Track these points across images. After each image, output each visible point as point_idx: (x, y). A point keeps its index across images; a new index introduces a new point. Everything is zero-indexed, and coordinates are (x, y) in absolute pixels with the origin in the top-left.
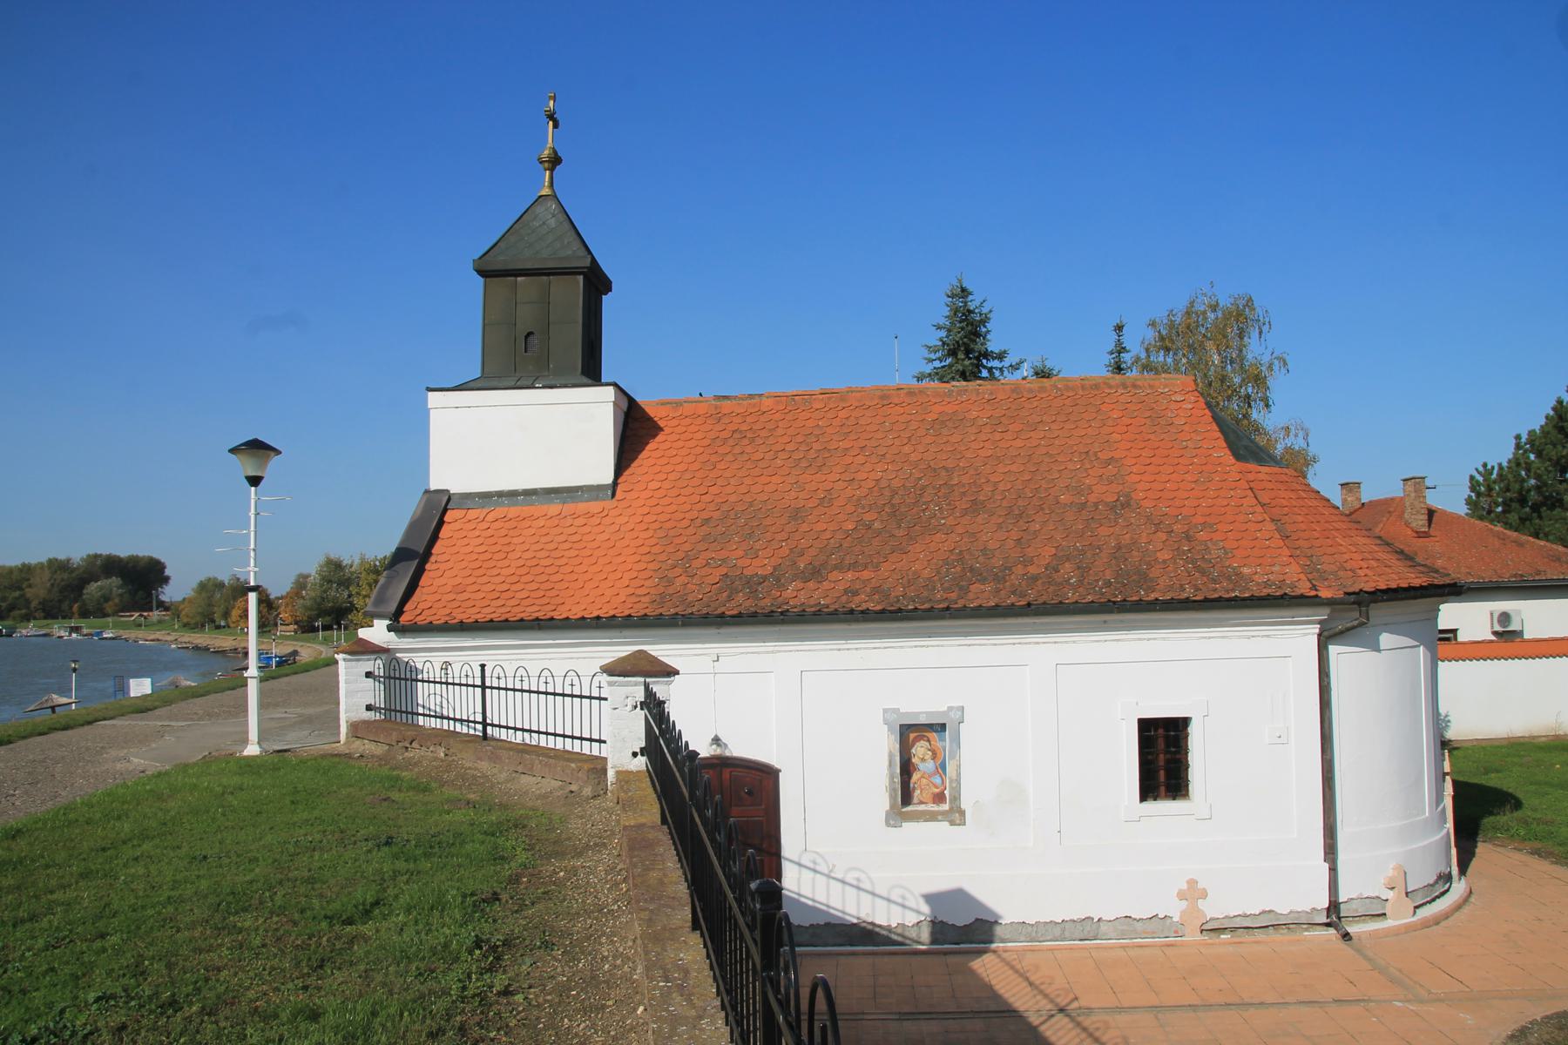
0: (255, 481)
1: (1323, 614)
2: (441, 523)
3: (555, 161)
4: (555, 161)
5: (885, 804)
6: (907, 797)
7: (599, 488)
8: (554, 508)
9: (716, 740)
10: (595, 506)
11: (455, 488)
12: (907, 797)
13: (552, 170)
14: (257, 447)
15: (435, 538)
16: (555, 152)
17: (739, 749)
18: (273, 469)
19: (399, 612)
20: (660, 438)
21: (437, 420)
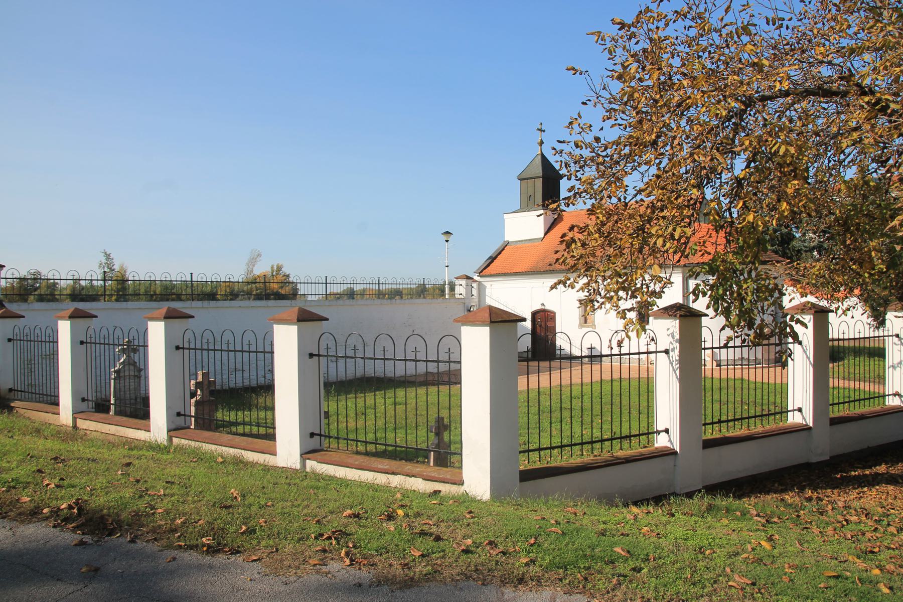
0: (447, 241)
1: (680, 270)
2: (503, 249)
3: (541, 143)
4: (541, 143)
5: (578, 323)
6: (586, 322)
7: (539, 238)
8: (530, 244)
9: (543, 304)
10: (536, 244)
11: (510, 240)
12: (586, 322)
13: (541, 146)
14: (447, 233)
15: (500, 253)
16: (541, 140)
17: (548, 307)
18: (451, 238)
19: (482, 272)
20: (563, 222)
21: (506, 221)
